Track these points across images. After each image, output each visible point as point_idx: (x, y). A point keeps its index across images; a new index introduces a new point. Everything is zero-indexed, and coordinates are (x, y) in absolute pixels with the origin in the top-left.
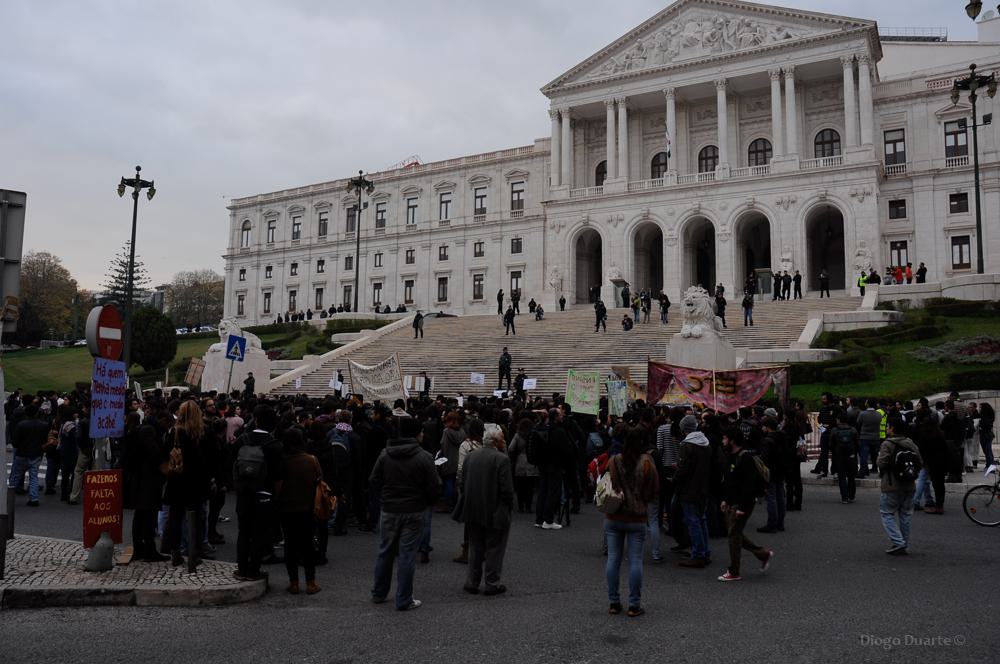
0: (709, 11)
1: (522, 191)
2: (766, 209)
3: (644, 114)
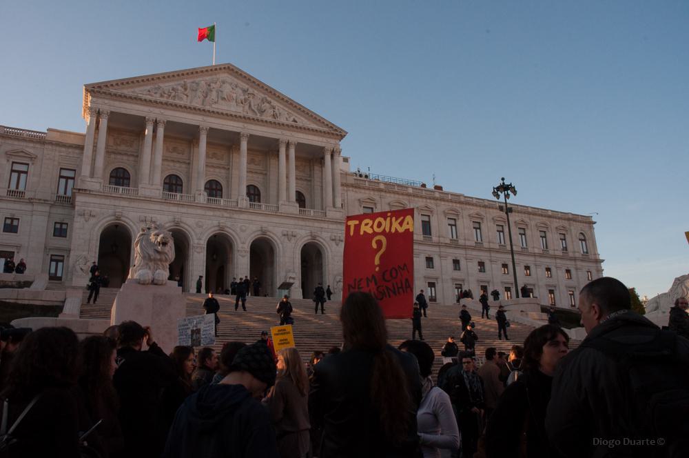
0: (239, 82)
1: (26, 173)
2: (275, 238)
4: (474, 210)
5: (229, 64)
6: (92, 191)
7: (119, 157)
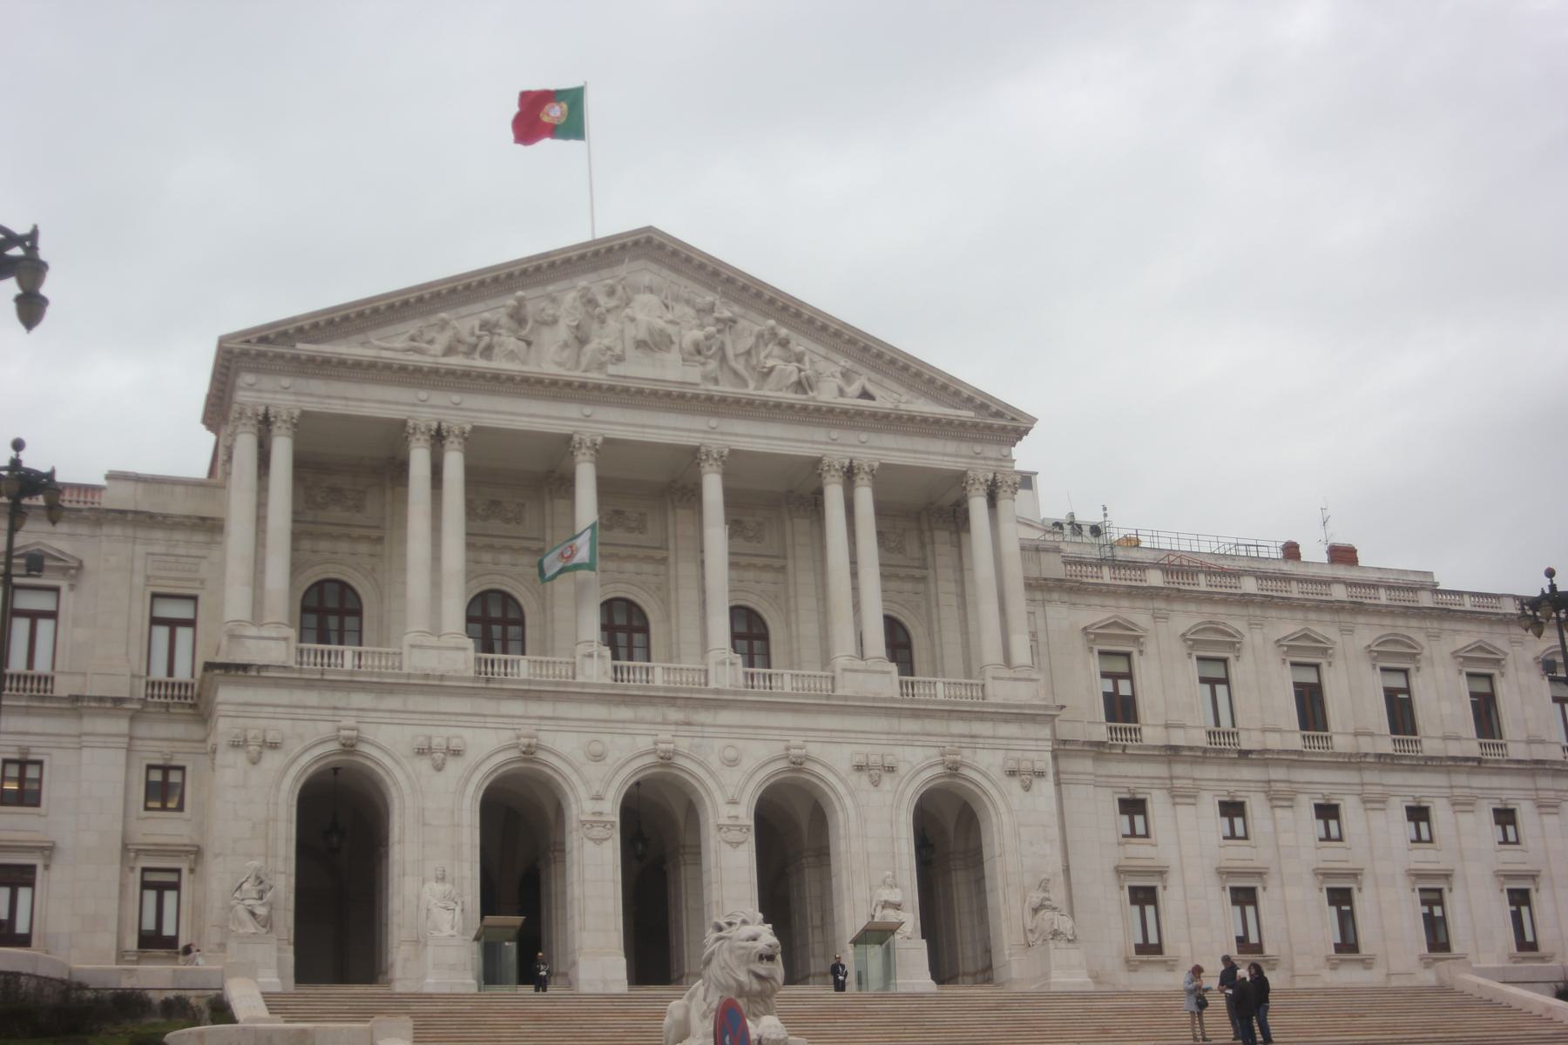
1: (52, 615)
3: (515, 486)
4: (1465, 637)
5: (650, 229)
6: (266, 667)
7: (324, 545)
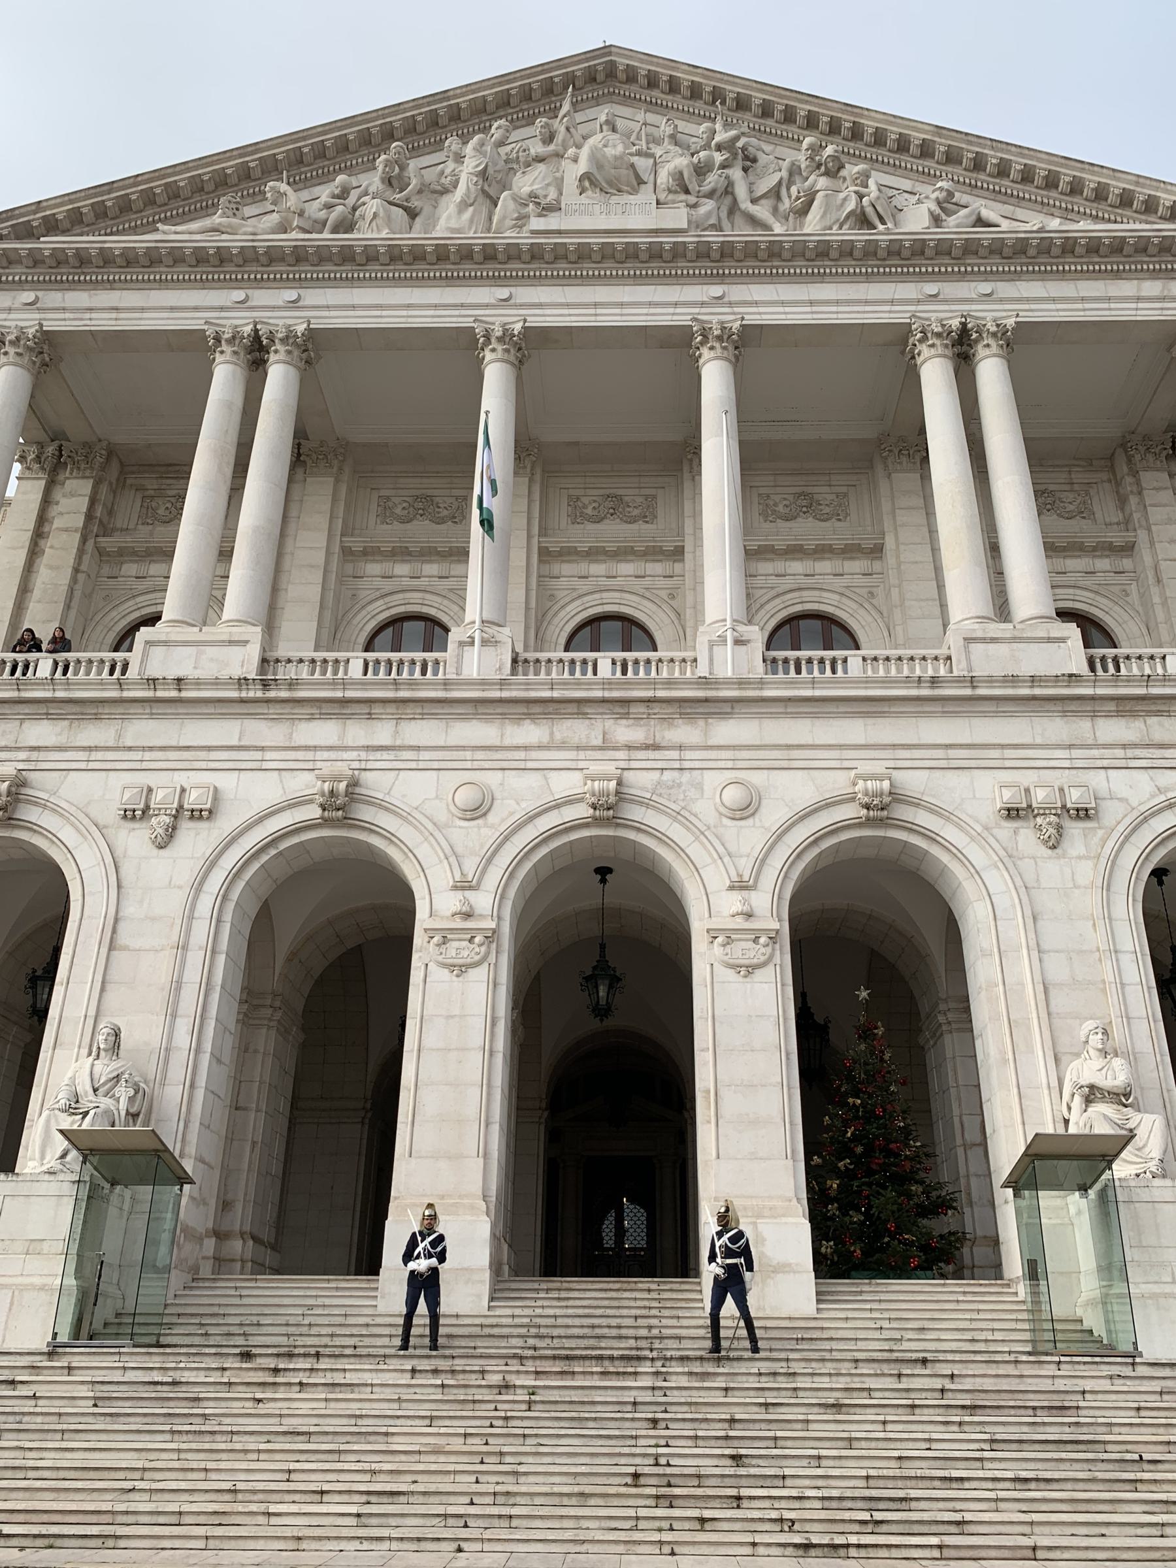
2: (949, 833)
5: (607, 50)
